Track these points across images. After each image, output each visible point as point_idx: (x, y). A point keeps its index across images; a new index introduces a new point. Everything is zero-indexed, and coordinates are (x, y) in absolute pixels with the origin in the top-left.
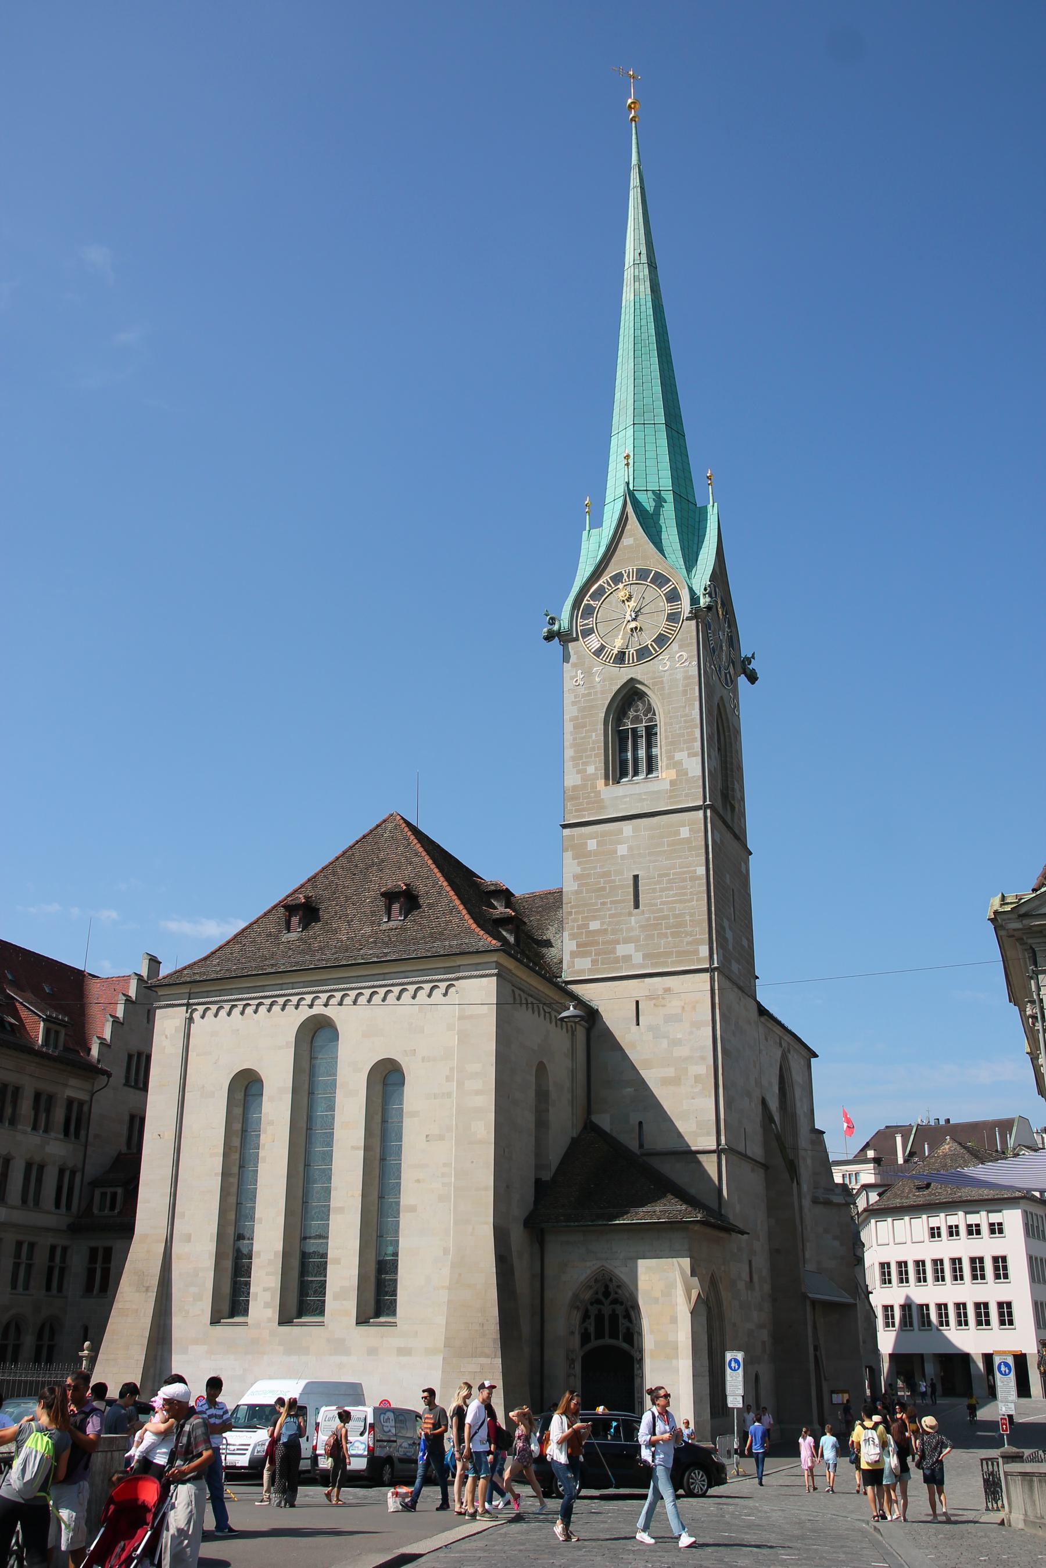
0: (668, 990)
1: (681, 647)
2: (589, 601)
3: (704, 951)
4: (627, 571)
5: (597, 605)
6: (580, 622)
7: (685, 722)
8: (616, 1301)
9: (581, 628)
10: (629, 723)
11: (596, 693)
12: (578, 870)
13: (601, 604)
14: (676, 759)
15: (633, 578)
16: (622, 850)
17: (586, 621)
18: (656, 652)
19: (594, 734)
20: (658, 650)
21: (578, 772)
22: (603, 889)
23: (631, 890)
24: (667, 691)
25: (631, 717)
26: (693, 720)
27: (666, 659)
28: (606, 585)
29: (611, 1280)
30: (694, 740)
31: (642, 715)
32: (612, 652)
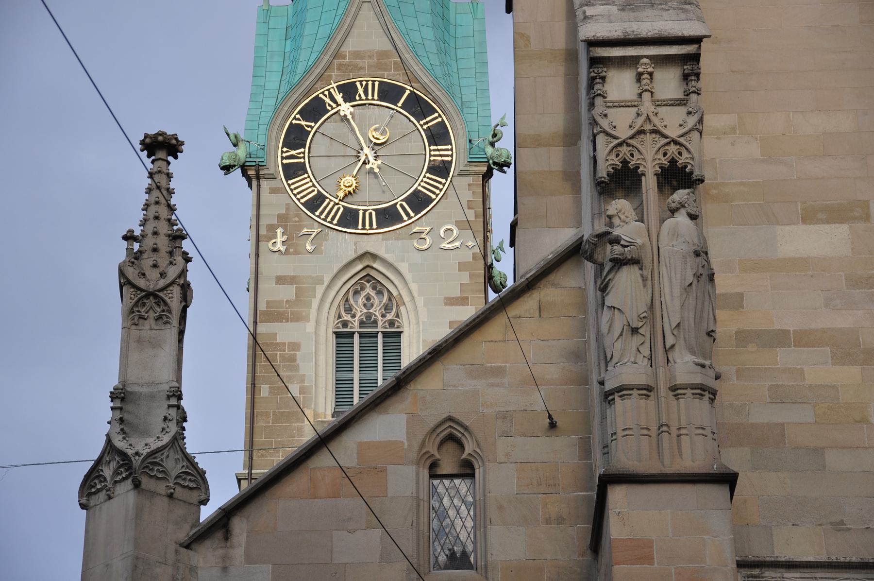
2: (298, 119)
4: (364, 83)
5: (312, 128)
6: (282, 152)
9: (285, 161)
10: (356, 324)
13: (318, 128)
15: (373, 95)
17: (293, 152)
18: (410, 217)
20: (412, 214)
25: (359, 314)
27: (426, 232)
28: (327, 100)
31: (377, 314)
32: (336, 207)
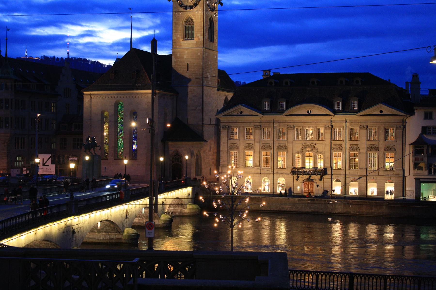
0: (194, 90)
1: (200, 7)
3: (201, 82)
7: (200, 27)
8: (178, 155)
11: (180, 16)
12: (175, 60)
14: (198, 36)
16: (185, 57)
19: (179, 27)
21: (176, 36)
22: (181, 66)
23: (187, 66)
24: (196, 18)
26: (202, 26)
29: (178, 151)
30: (202, 31)
